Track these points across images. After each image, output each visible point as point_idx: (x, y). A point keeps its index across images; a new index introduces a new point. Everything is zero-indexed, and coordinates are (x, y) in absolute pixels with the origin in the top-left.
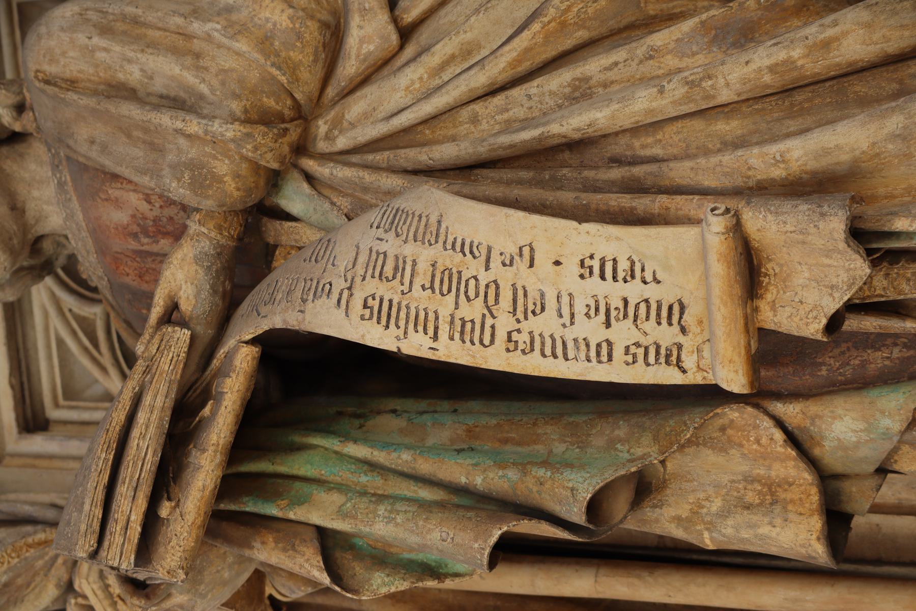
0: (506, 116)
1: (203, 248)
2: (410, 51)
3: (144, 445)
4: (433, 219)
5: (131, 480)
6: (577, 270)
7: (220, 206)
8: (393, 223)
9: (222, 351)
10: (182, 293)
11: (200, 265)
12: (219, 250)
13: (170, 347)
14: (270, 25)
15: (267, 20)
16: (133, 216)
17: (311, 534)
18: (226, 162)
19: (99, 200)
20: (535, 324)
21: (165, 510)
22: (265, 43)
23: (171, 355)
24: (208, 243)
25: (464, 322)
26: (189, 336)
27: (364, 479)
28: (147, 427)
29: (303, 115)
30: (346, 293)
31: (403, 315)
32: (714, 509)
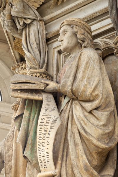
0: (75, 133)
2: (87, 114)
4: (53, 127)
6: (47, 152)
8: (54, 120)
14: (87, 91)
15: (88, 91)
17: (22, 112)
20: (41, 146)
21: (19, 91)
22: (84, 91)
25: (41, 135)
27: (32, 118)
29: (77, 99)
30: (45, 115)
31: (42, 125)
32: (30, 173)
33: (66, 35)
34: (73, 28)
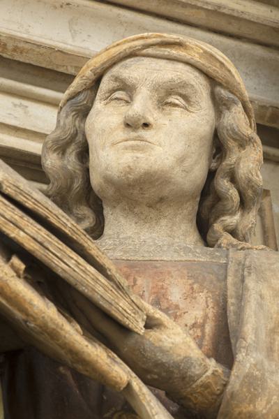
1: (195, 367)
3: (72, 263)
5: (50, 242)
7: (232, 395)
9: (115, 356)
10: (165, 336)
11: (183, 360)
12: (187, 379)
13: (134, 313)
16: (177, 307)
18: (264, 411)
19: (190, 282)
23: (129, 312)
24: (197, 372)
26: (139, 332)
28: (84, 271)
33: (177, 112)
34: (220, 105)
